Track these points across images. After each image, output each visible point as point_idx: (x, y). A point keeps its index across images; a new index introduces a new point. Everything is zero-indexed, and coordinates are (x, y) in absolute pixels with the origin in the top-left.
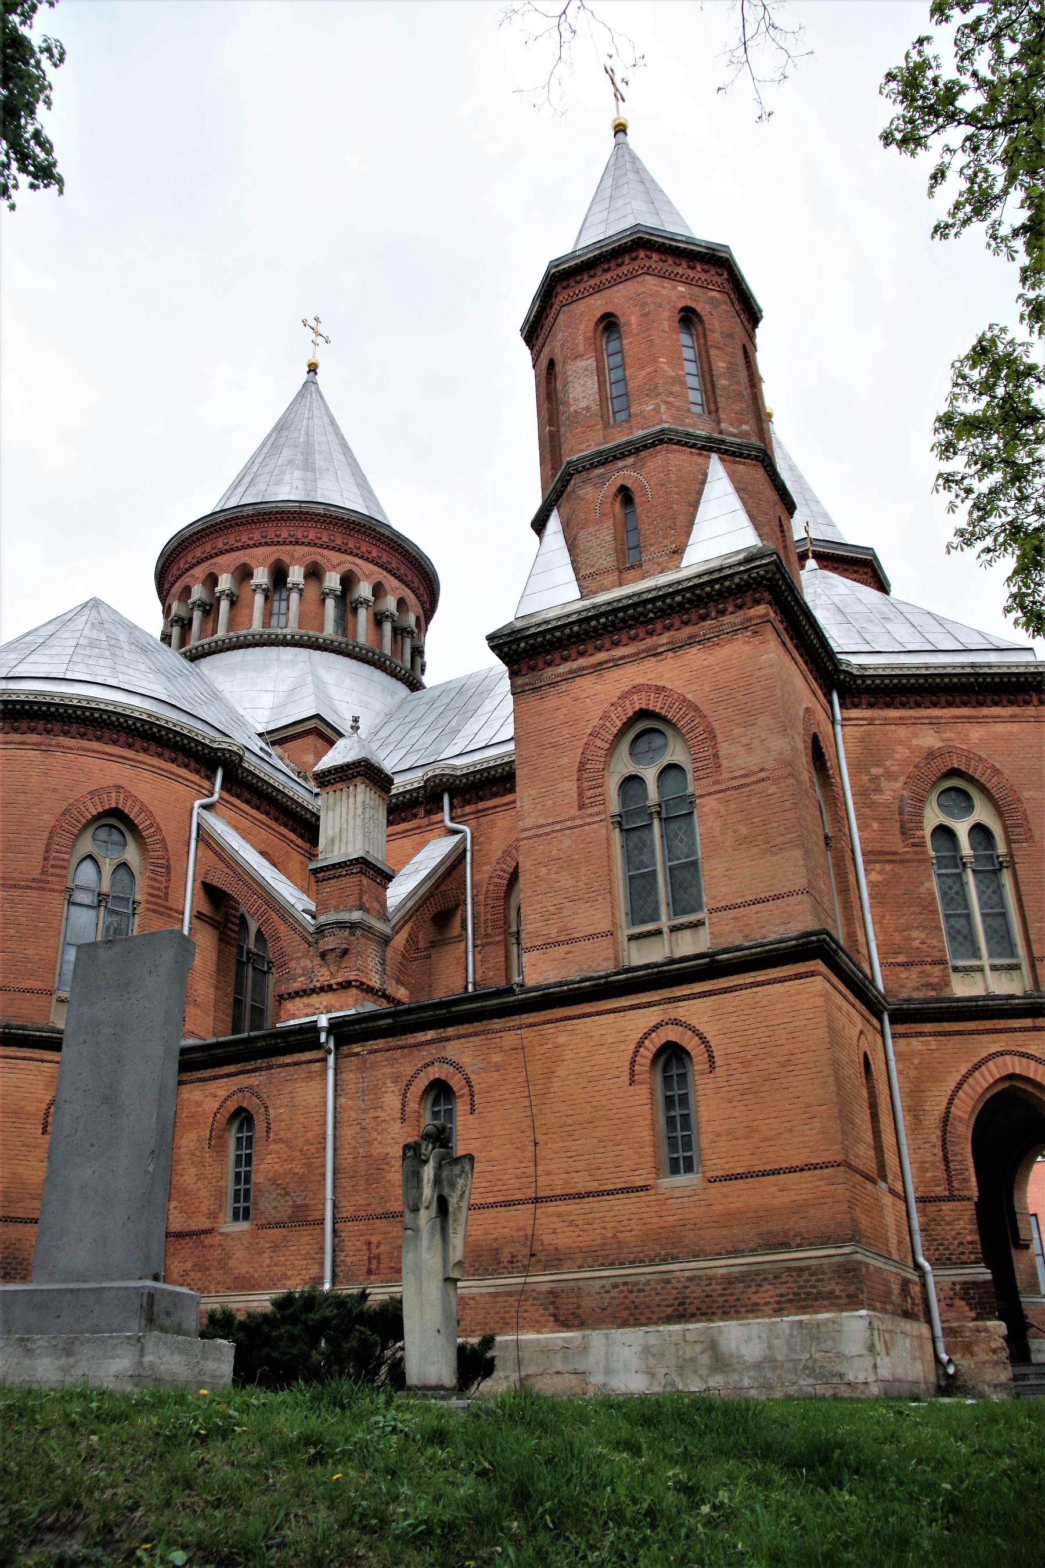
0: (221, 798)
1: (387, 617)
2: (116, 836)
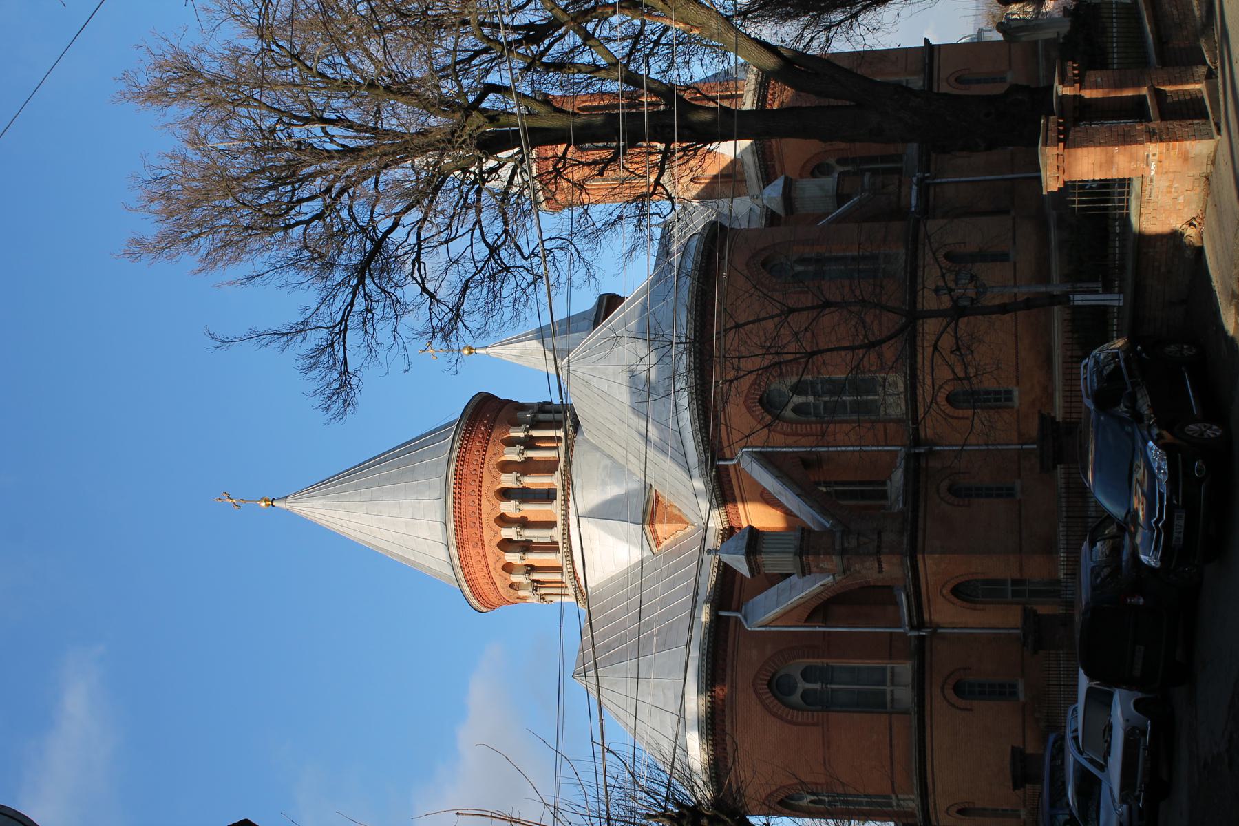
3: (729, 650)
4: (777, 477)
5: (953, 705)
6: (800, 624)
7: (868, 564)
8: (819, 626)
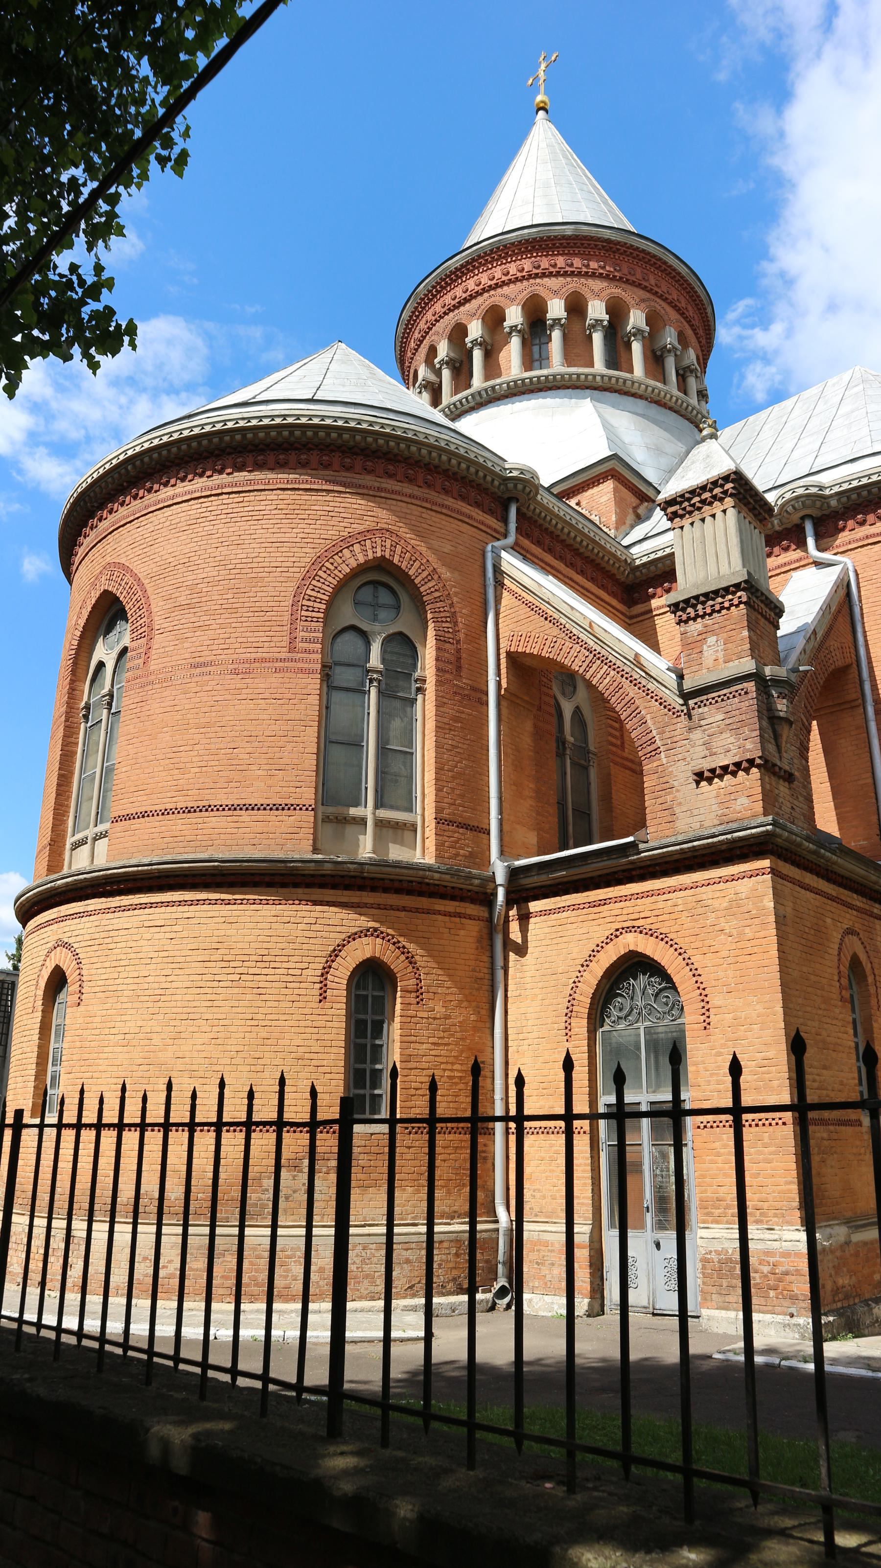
0: (516, 543)
1: (669, 351)
2: (385, 597)
3: (450, 501)
4: (829, 606)
5: (335, 954)
6: (503, 644)
7: (728, 739)
8: (499, 684)
